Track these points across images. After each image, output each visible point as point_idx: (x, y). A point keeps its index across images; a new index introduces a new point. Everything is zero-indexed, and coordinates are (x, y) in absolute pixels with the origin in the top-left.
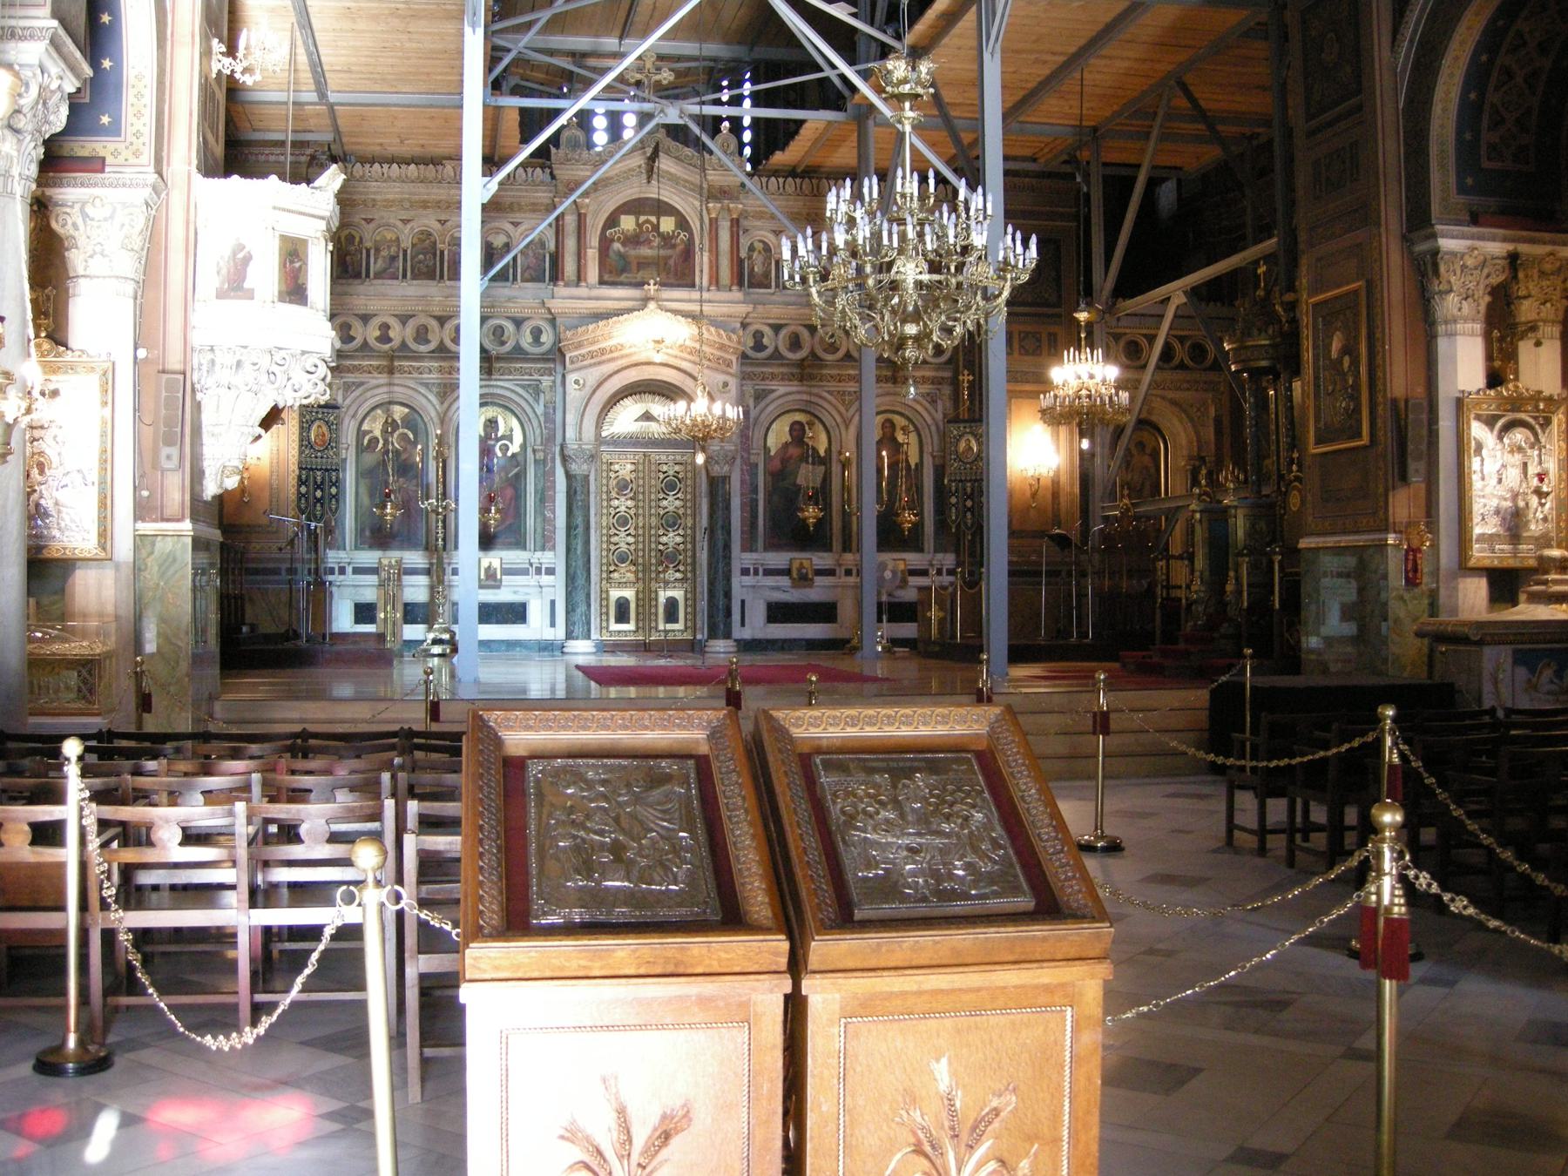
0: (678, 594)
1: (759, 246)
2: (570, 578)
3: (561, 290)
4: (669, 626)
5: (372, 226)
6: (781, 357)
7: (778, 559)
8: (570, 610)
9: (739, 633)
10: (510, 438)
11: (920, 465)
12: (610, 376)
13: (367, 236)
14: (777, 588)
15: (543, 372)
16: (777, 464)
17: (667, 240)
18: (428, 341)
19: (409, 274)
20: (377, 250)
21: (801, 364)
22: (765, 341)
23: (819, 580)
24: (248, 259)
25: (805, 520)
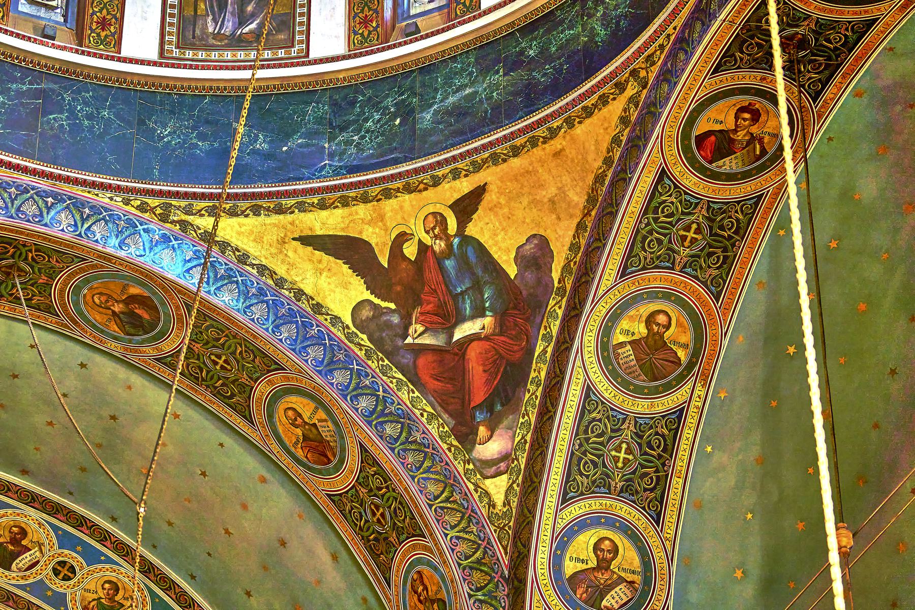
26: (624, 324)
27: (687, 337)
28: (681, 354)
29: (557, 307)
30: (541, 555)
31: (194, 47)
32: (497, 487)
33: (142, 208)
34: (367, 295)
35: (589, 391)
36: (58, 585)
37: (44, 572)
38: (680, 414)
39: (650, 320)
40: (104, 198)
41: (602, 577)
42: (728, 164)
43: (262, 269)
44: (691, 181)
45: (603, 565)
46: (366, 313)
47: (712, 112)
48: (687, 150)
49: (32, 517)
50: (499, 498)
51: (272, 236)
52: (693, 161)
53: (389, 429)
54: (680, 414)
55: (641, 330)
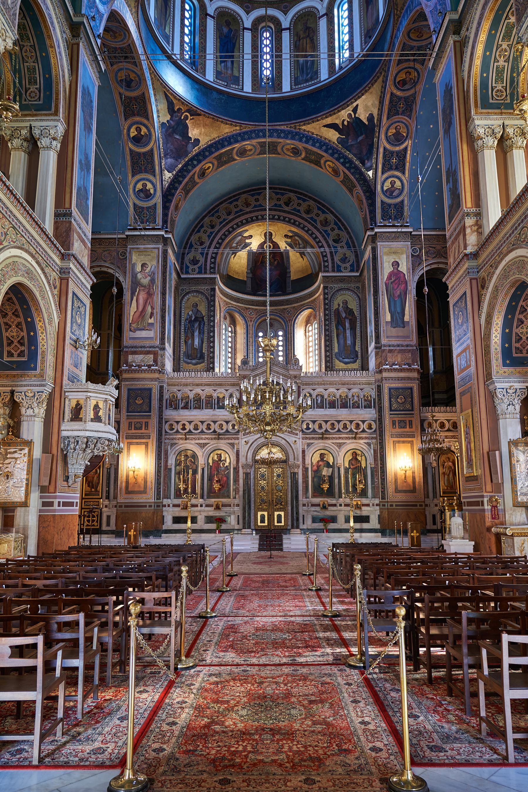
0: (282, 514)
1: (308, 395)
2: (244, 508)
5: (180, 392)
7: (317, 500)
8: (244, 518)
9: (302, 526)
10: (225, 461)
11: (366, 468)
14: (316, 511)
16: (315, 468)
20: (182, 400)
21: (322, 434)
22: (310, 426)
23: (331, 508)
24: (81, 408)
25: (323, 488)
26: (390, 131)
27: (406, 130)
28: (405, 134)
29: (377, 129)
30: (379, 187)
31: (298, 85)
32: (370, 173)
33: (291, 127)
34: (339, 136)
35: (385, 149)
36: (298, 208)
37: (295, 206)
38: (406, 149)
39: (396, 128)
40: (282, 127)
41: (393, 189)
42: (406, 87)
43: (317, 135)
44: (399, 93)
45: (393, 186)
46: (339, 140)
47: (399, 75)
48: (396, 86)
49: (292, 195)
50: (371, 176)
51: (318, 127)
52: (398, 88)
53: (347, 165)
54: (406, 149)
55: (394, 131)
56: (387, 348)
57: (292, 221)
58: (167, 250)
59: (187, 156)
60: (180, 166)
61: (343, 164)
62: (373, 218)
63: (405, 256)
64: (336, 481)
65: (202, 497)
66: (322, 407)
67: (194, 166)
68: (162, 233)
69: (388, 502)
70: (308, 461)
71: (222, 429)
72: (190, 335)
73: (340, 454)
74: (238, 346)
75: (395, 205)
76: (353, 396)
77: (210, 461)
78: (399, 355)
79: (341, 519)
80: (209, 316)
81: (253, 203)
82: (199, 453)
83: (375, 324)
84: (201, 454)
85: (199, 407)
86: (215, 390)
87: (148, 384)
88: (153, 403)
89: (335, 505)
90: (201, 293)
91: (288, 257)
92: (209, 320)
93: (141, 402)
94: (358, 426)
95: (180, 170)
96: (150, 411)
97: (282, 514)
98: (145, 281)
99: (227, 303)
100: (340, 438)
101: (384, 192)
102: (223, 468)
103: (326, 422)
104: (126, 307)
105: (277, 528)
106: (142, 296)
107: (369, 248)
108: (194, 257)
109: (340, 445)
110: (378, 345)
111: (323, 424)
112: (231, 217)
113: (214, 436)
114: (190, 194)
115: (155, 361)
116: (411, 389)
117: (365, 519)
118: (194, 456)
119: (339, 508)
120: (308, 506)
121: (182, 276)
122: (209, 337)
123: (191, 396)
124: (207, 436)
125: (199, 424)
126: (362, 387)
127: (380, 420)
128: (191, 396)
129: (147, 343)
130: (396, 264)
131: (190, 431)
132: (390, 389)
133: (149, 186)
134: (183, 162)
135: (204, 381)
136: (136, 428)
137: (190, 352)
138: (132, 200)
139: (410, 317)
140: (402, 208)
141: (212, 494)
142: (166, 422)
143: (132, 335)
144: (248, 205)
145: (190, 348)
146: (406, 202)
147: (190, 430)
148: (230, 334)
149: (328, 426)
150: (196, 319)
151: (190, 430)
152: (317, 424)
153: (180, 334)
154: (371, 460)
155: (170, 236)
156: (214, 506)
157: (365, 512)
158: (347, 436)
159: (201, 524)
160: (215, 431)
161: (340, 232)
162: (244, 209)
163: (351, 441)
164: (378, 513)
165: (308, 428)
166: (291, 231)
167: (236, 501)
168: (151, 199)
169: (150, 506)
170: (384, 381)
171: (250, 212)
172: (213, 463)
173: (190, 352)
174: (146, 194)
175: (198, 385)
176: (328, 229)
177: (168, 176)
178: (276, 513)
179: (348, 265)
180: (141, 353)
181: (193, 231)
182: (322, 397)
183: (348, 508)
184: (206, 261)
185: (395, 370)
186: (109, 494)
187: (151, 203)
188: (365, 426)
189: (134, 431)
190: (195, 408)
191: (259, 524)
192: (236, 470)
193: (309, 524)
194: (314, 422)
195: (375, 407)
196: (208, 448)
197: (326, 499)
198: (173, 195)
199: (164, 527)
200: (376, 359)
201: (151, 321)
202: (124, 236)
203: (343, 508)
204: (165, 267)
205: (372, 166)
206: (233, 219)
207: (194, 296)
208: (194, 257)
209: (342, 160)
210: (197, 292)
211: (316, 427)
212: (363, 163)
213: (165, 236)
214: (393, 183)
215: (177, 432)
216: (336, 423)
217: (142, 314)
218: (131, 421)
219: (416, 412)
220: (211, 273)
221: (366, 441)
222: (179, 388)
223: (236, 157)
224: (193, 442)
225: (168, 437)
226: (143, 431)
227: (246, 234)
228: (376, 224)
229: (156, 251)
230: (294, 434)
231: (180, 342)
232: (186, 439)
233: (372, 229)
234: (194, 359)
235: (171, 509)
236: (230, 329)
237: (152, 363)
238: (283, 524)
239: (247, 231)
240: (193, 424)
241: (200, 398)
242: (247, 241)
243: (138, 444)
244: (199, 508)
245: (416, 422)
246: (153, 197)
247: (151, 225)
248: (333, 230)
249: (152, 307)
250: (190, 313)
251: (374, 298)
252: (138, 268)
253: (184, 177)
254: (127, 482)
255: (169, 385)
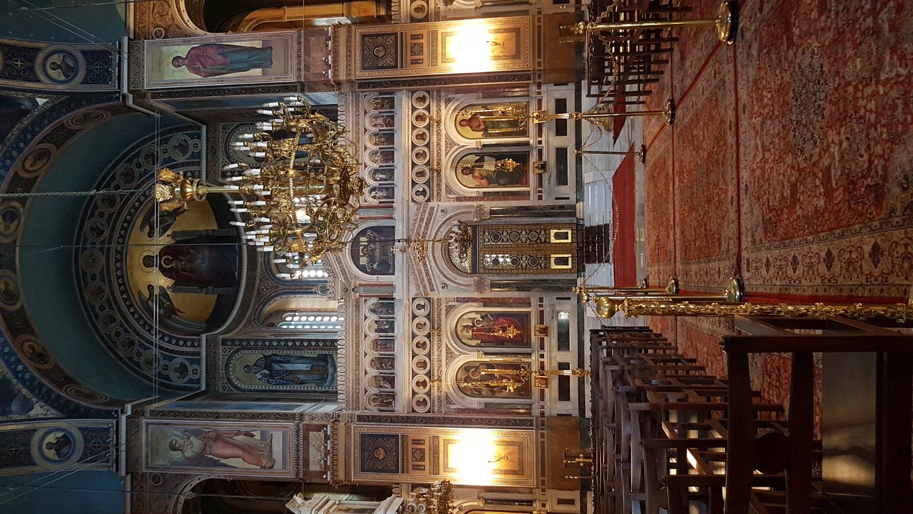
0: (553, 232)
1: (373, 193)
3: (395, 295)
4: (570, 236)
5: (369, 389)
6: (428, 181)
7: (532, 178)
8: (561, 289)
12: (440, 270)
13: (375, 392)
15: (439, 305)
16: (484, 182)
17: (370, 242)
18: (425, 362)
19: (392, 371)
21: (431, 170)
22: (421, 189)
30: (60, 88)
32: (41, 101)
41: (63, 67)
45: (59, 67)
49: (87, 226)
50: (45, 100)
53: (29, 136)
56: (303, 73)
57: (125, 225)
58: (152, 411)
59: (8, 382)
60: (24, 391)
61: (27, 142)
62: (109, 96)
63: (165, 48)
64: (504, 150)
65: (530, 355)
66: (390, 172)
67: (25, 369)
68: (123, 418)
69: (534, 70)
70: (473, 192)
71: (425, 324)
72: (290, 377)
73: (462, 144)
74: (317, 307)
75: (89, 63)
76: (375, 125)
77: (474, 342)
78: (313, 55)
79: (560, 141)
80: (264, 347)
81: (98, 283)
82: (461, 360)
83: (268, 92)
84: (463, 356)
85: (392, 360)
86: (366, 336)
87: (355, 440)
88: (383, 432)
89: (540, 152)
90: (228, 359)
91: (184, 233)
92: (270, 347)
93: (382, 451)
94: (420, 118)
95: (31, 389)
96: (396, 437)
97: (553, 232)
98: (197, 444)
99: (249, 322)
100: (438, 144)
101: (69, 79)
102: (485, 324)
103: (414, 165)
104: (238, 475)
105: (575, 240)
106: (220, 449)
107: (153, 102)
108: (176, 370)
109: (450, 143)
110: (299, 88)
111: (416, 169)
112: (118, 316)
113: (436, 337)
114: (72, 375)
115: (319, 428)
116: (364, 36)
117: (561, 105)
118: (467, 368)
119: (543, 144)
120: (541, 192)
121: (204, 388)
122: (295, 347)
123: (374, 372)
124: (436, 348)
125: (416, 359)
126: (362, 113)
127: (412, 83)
128: (374, 372)
129: (292, 441)
130: (177, 61)
131: (429, 374)
132: (364, 68)
133: (51, 438)
134: (20, 386)
135: (351, 352)
136: (422, 459)
137: (317, 377)
138: (73, 465)
139: (255, 39)
140: (93, 52)
141: (523, 340)
142: (414, 411)
143: (278, 465)
144: (100, 291)
145: (311, 377)
146: (85, 47)
147: (426, 375)
148: (296, 319)
149: (420, 162)
150: (268, 367)
151: (426, 375)
152: (416, 180)
153: (289, 391)
154: (471, 99)
155: (129, 407)
156: (542, 335)
157: (549, 105)
158: (435, 133)
159: (570, 357)
160: (428, 336)
161: (143, 154)
162: (105, 297)
163: (442, 128)
164: (551, 87)
165: (423, 193)
166: (142, 228)
167: (534, 301)
168: (72, 435)
169: (543, 436)
170: (353, 78)
171: (111, 287)
172: (477, 339)
173: (317, 377)
174: (63, 444)
175: (358, 362)
176: (137, 171)
177: (38, 410)
178: (553, 240)
179: (191, 142)
180: (306, 451)
181: (136, 372)
182: (376, 171)
183: (544, 130)
184: (182, 353)
185: (335, 60)
186: (524, 501)
187: (78, 437)
188: (421, 109)
189: (427, 463)
190: (392, 366)
191: (570, 267)
192: (486, 302)
193: (568, 190)
194: (414, 184)
195: (392, 93)
196: (454, 345)
197: (531, 164)
198: (68, 401)
199: (576, 413)
200: (320, 90)
201: (258, 436)
202: (129, 477)
203: (543, 139)
204: (177, 415)
205: (30, 99)
206: (121, 313)
207: (234, 371)
208: (176, 370)
209: (22, 145)
210: (227, 365)
211: (421, 181)
212: (27, 112)
213: (129, 413)
214: (55, 66)
215: (429, 394)
216: (416, 151)
217: (247, 449)
218: (410, 467)
219: (398, 30)
220: (200, 345)
221: (443, 105)
222: (362, 391)
223: (17, 306)
224: (444, 369)
225: (436, 409)
226: (426, 447)
227: (146, 294)
228: (115, 92)
229: (150, 427)
230: (431, 214)
231: (302, 392)
232: (440, 380)
233: (124, 97)
234: (327, 370)
235: (547, 403)
236: (289, 319)
237: (322, 434)
238: (570, 232)
239: (140, 293)
240: (416, 370)
241: (378, 359)
242: (156, 292)
243: (446, 456)
244: (545, 360)
245: (416, 28)
246: (68, 432)
247: (111, 435)
248: (139, 165)
249: (236, 435)
250: (259, 376)
251: (228, 94)
252: (177, 455)
253: (41, 385)
254: (506, 472)
255: (357, 408)
